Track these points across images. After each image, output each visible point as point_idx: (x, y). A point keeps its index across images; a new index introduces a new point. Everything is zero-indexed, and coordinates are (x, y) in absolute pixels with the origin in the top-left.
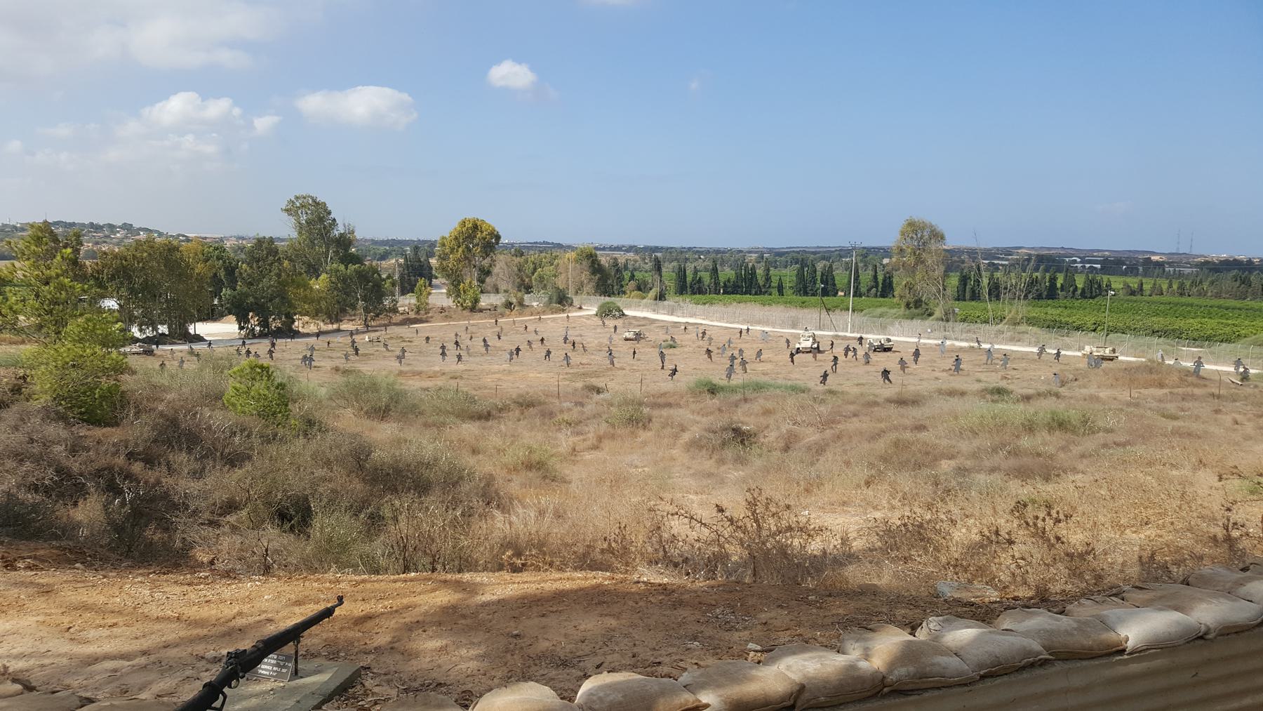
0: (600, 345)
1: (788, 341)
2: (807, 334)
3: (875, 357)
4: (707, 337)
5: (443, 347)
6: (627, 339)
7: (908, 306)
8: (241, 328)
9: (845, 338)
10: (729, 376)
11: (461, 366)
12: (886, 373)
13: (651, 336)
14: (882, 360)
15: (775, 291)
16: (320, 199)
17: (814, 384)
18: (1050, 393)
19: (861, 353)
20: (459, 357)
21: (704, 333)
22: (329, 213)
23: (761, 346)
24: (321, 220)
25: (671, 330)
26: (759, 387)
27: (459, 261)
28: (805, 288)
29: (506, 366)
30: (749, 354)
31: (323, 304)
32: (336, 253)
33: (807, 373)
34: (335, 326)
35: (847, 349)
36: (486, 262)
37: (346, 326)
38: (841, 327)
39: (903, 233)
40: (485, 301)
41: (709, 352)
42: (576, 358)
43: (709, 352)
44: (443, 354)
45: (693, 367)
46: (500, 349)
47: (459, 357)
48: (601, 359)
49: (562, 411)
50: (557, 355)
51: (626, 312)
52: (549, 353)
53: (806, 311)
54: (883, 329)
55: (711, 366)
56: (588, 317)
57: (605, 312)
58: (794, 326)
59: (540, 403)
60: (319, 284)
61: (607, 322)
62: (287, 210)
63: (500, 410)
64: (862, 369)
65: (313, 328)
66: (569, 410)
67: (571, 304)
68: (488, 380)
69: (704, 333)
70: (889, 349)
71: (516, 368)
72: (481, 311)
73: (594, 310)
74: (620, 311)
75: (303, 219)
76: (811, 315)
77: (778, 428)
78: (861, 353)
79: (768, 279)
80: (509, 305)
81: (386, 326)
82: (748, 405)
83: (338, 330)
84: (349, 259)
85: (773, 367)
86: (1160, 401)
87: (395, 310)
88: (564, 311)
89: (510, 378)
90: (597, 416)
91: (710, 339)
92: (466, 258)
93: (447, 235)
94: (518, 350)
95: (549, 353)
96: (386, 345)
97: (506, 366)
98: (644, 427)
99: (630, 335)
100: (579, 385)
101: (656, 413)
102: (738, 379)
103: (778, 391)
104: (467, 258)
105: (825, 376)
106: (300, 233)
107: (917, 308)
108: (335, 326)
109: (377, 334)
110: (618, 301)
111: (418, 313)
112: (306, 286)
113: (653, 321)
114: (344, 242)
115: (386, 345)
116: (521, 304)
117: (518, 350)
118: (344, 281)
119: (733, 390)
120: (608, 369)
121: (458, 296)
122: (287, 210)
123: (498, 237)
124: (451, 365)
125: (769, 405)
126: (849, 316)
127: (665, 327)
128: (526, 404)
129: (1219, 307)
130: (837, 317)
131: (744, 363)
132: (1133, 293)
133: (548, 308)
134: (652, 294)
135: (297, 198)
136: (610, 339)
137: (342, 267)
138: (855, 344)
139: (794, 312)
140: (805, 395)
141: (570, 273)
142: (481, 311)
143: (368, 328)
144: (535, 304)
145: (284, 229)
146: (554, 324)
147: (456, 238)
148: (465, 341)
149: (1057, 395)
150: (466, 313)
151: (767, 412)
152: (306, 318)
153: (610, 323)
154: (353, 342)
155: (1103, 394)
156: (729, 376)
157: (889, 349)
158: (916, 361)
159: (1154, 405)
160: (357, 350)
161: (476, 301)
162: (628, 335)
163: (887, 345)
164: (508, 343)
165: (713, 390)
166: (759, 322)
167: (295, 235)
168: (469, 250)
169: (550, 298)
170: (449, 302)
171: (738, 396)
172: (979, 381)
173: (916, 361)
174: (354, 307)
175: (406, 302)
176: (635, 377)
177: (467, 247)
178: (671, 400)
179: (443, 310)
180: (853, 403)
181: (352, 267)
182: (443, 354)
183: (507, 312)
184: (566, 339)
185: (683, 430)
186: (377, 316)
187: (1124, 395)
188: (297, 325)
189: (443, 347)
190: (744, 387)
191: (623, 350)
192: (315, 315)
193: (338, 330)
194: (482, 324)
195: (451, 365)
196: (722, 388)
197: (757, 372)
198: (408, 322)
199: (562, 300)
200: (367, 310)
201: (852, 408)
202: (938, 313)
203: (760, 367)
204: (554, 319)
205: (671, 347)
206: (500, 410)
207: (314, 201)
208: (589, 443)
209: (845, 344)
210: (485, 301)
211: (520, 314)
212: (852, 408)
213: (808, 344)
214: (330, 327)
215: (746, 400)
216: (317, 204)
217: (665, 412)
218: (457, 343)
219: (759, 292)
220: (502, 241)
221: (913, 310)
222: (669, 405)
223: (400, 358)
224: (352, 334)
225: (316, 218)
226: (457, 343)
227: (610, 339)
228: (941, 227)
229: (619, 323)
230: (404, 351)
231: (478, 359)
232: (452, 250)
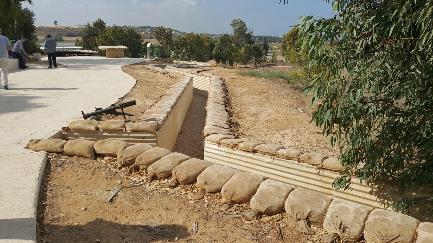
16: (243, 21)
22: (245, 26)
24: (243, 28)
62: (232, 25)
87: (265, 60)
106: (235, 33)
111: (272, 62)
112: (237, 51)
114: (249, 36)
122: (232, 25)
135: (235, 20)
137: (249, 45)
143: (257, 67)
145: (230, 31)
147: (290, 35)
167: (233, 34)
170: (284, 59)
177: (294, 38)
181: (252, 45)
186: (259, 63)
193: (246, 67)
198: (269, 65)
200: (256, 60)
207: (241, 21)
214: (244, 66)
216: (242, 22)
225: (240, 27)
232: (288, 39)
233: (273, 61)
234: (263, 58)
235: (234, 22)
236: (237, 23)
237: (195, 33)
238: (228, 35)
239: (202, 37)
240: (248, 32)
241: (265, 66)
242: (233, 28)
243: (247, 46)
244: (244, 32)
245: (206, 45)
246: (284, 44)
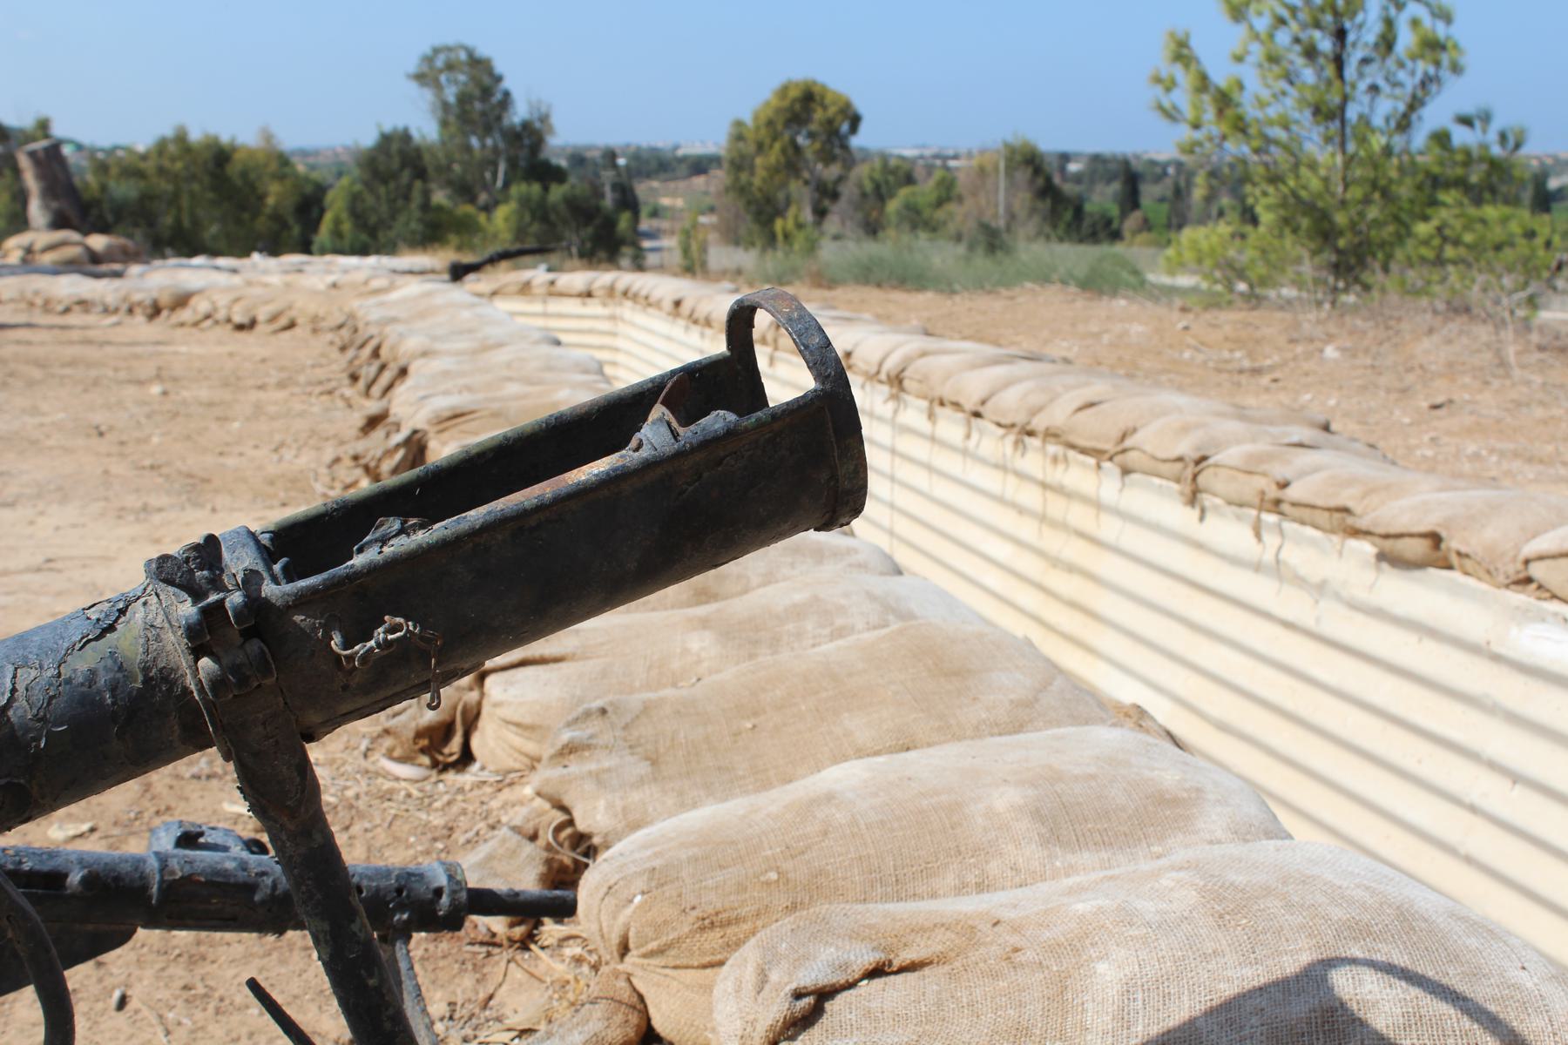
16: (483, 51)
22: (499, 79)
24: (486, 93)
36: (833, 171)
51: (1151, 277)
62: (420, 78)
74: (1136, 272)
75: (451, 94)
93: (748, 118)
104: (792, 163)
106: (444, 124)
114: (530, 137)
123: (855, 121)
135: (436, 51)
137: (536, 188)
141: (1004, 199)
147: (770, 123)
168: (797, 149)
207: (470, 53)
225: (475, 93)
232: (760, 147)
235: (429, 60)
236: (450, 67)
237: (195, 136)
238: (406, 136)
239: (237, 156)
242: (428, 95)
244: (499, 118)
245: (271, 201)
246: (744, 177)
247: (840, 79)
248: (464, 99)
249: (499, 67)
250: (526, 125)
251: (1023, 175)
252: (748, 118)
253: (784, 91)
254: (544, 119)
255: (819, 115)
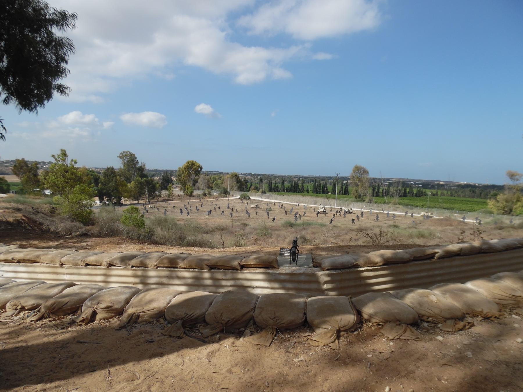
0: (242, 210)
1: (314, 209)
2: (322, 206)
3: (348, 215)
4: (283, 207)
5: (181, 210)
6: (252, 208)
7: (356, 197)
8: (101, 202)
9: (335, 209)
10: (296, 221)
11: (189, 217)
12: (353, 220)
13: (261, 207)
14: (350, 216)
15: (306, 192)
16: (133, 153)
17: (328, 223)
18: (413, 227)
19: (342, 214)
20: (188, 213)
21: (282, 206)
22: (136, 158)
23: (304, 211)
24: (133, 161)
25: (269, 205)
26: (309, 224)
27: (186, 177)
28: (317, 190)
29: (207, 217)
30: (301, 213)
31: (132, 193)
32: (138, 174)
33: (325, 220)
34: (137, 202)
35: (337, 212)
36: (196, 177)
37: (141, 202)
38: (333, 204)
39: (354, 171)
40: (195, 193)
41: (286, 212)
42: (234, 215)
43: (286, 212)
44: (182, 212)
45: (281, 219)
46: (202, 211)
47: (188, 213)
48: (243, 215)
49: (236, 232)
50: (227, 213)
51: (251, 198)
52: (223, 212)
53: (319, 199)
54: (347, 206)
55: (287, 218)
56: (236, 199)
57: (243, 198)
58: (315, 204)
59: (226, 229)
60: (131, 185)
61: (244, 201)
62: (119, 157)
63: (211, 232)
64: (344, 219)
65: (128, 202)
66: (239, 231)
67: (229, 194)
68: (201, 222)
69: (282, 206)
70: (351, 213)
71: (210, 218)
72: (194, 196)
73: (238, 197)
75: (126, 160)
76: (321, 200)
77: (320, 238)
78: (342, 214)
79: (303, 187)
80: (205, 194)
81: (157, 202)
82: (305, 231)
83: (138, 203)
84: (143, 176)
85: (310, 217)
86: (452, 230)
87: (160, 196)
88: (226, 197)
89: (210, 221)
90: (251, 233)
91: (285, 208)
92: (189, 176)
93: (181, 167)
94: (211, 211)
95: (223, 212)
96: (158, 209)
97: (207, 217)
98: (272, 238)
99: (253, 206)
100: (239, 224)
101: (273, 232)
102: (299, 222)
103: (316, 226)
105: (331, 221)
106: (124, 166)
107: (360, 198)
108: (137, 202)
109: (153, 205)
110: (248, 194)
111: (169, 197)
112: (126, 186)
113: (262, 201)
114: (141, 170)
115: (158, 209)
116: (209, 194)
117: (211, 211)
118: (141, 184)
119: (299, 225)
120: (247, 218)
121: (185, 190)
122: (119, 157)
123: (201, 168)
124: (185, 216)
125: (314, 230)
126: (336, 201)
127: (267, 203)
128: (222, 229)
129: (465, 201)
130: (331, 201)
131: (300, 216)
132: (434, 195)
133: (220, 196)
134: (261, 191)
135: (124, 152)
136: (246, 207)
137: (140, 179)
138: (339, 210)
139: (315, 199)
140: (325, 228)
141: (228, 183)
142: (194, 196)
143: (150, 203)
144: (215, 194)
145: (118, 165)
146: (223, 202)
147: (185, 168)
148: (189, 208)
149: (415, 228)
150: (188, 197)
151: (314, 233)
152: (126, 199)
153: (245, 202)
154: (145, 207)
155: (432, 228)
156: (296, 221)
157: (351, 213)
158: (362, 217)
159: (451, 231)
160: (147, 210)
161: (192, 193)
162: (253, 206)
163: (351, 211)
164: (206, 208)
165: (291, 225)
166: (302, 202)
167: (122, 167)
168: (190, 173)
169: (221, 192)
170: (181, 193)
171: (301, 228)
172: (386, 223)
173: (362, 217)
174: (144, 194)
175: (164, 193)
176: (257, 221)
178: (277, 228)
179: (179, 196)
180: (343, 230)
181: (144, 179)
182: (182, 212)
183: (204, 197)
184: (228, 207)
185: (286, 238)
186: (153, 198)
187: (440, 228)
188: (123, 201)
189: (181, 210)
190: (303, 224)
191: (251, 211)
192: (129, 197)
193: (138, 203)
194: (195, 201)
195: (185, 216)
196: (295, 225)
197: (305, 219)
199: (225, 193)
200: (149, 196)
201: (344, 232)
202: (367, 200)
203: (306, 218)
204: (223, 200)
205: (270, 211)
206: (211, 232)
207: (130, 153)
208: (252, 242)
209: (336, 210)
210: (195, 193)
211: (209, 198)
212: (344, 232)
213: (322, 210)
214: (135, 202)
215: (304, 229)
216: (131, 155)
217: (276, 232)
218: (186, 208)
219: (300, 192)
220: (202, 170)
221: (358, 199)
222: (276, 230)
223: (165, 213)
224: (144, 205)
225: (130, 160)
226: (186, 208)
227: (246, 207)
228: (368, 168)
229: (249, 201)
230: (166, 211)
231: (195, 214)
232: (183, 172)
233: (169, 196)
234: (157, 193)
235: (121, 154)
236: (126, 155)
238: (113, 168)
240: (140, 165)
241: (160, 201)
242: (121, 161)
243: (138, 180)
247: (200, 161)
248: (128, 161)
249: (136, 156)
250: (141, 167)
251: (234, 179)
252: (181, 167)
253: (188, 162)
254: (144, 166)
255: (194, 167)
